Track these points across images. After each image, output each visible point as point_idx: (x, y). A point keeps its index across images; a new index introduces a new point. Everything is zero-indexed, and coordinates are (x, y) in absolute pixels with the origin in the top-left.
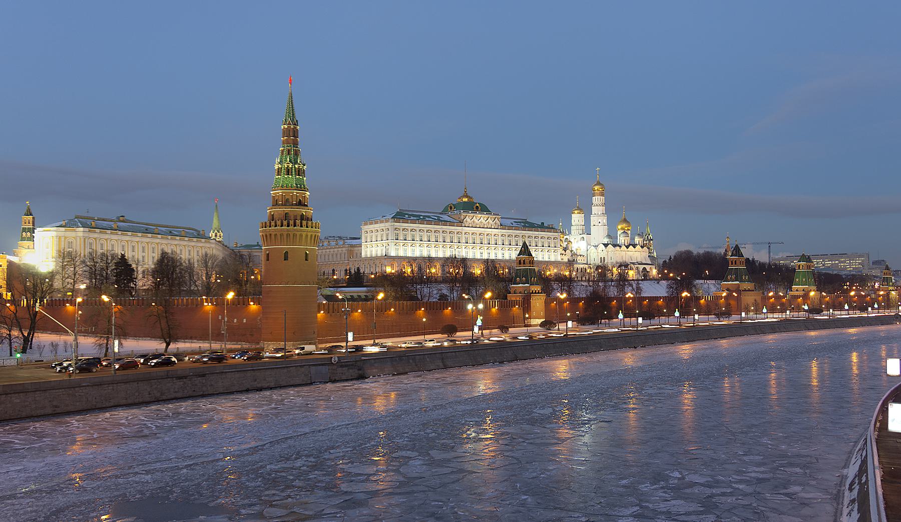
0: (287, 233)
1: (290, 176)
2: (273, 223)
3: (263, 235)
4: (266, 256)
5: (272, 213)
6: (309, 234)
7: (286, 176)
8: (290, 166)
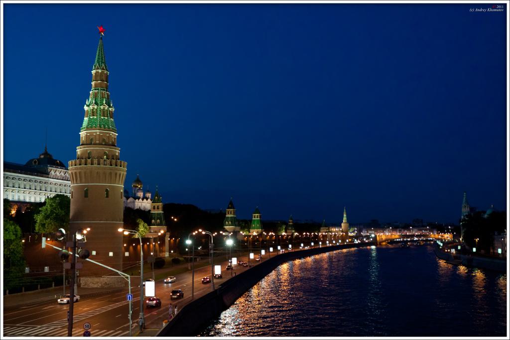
0: (110, 171)
1: (106, 118)
2: (95, 161)
3: (72, 173)
4: (83, 193)
5: (89, 151)
6: (122, 173)
7: (102, 117)
8: (106, 109)
